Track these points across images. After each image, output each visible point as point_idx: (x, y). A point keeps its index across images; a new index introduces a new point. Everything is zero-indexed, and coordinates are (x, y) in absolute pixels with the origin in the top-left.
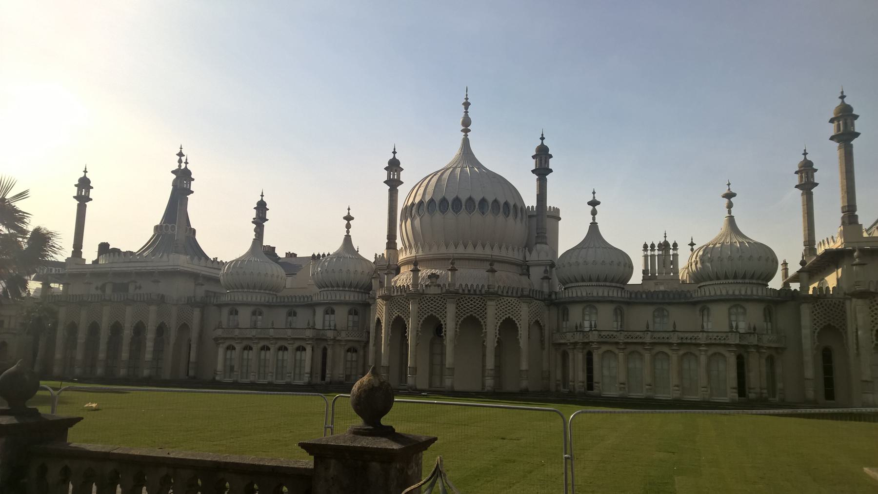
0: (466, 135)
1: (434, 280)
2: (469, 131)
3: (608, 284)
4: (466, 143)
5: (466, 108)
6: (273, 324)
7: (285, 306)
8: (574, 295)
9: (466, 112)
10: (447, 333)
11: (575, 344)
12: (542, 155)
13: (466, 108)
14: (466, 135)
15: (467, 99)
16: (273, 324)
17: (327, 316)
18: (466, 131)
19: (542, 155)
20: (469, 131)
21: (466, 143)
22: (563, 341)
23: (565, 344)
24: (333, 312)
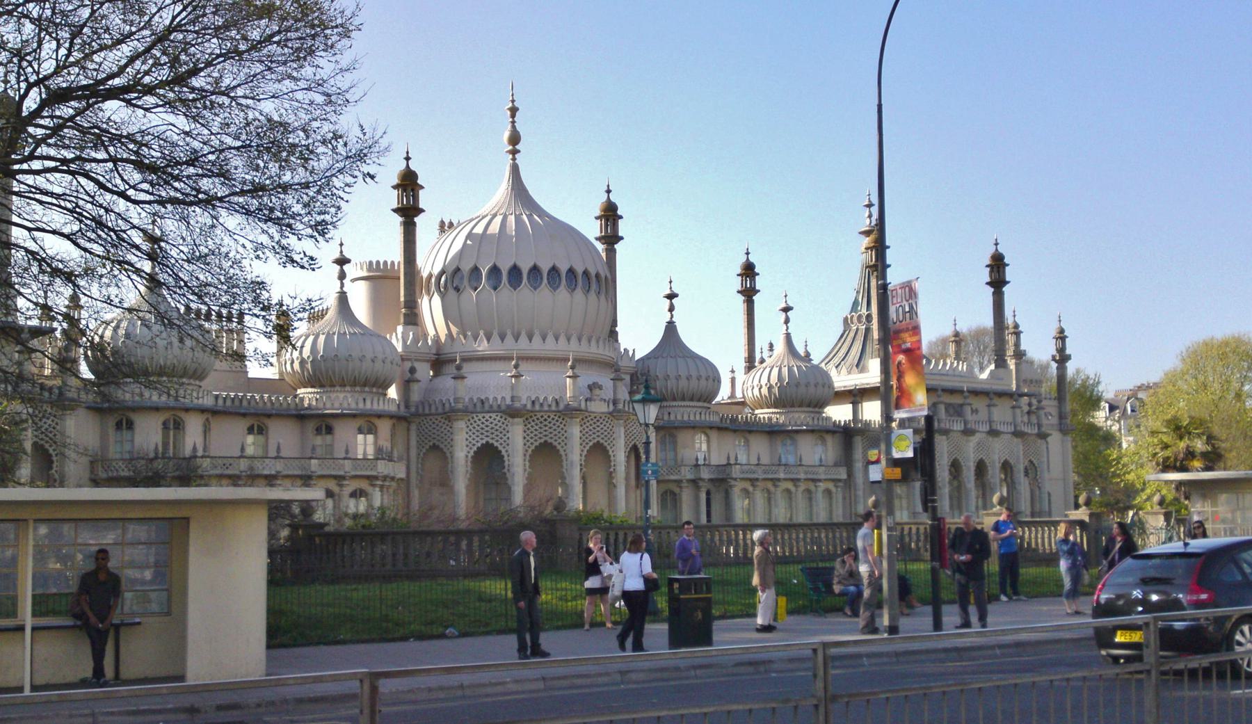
0: (514, 159)
1: (597, 392)
2: (519, 151)
3: (700, 404)
4: (515, 170)
5: (513, 116)
6: (347, 452)
7: (244, 415)
8: (679, 418)
9: (513, 122)
10: (618, 468)
11: (695, 482)
12: (610, 214)
13: (513, 116)
14: (514, 159)
15: (513, 101)
16: (347, 452)
17: (360, 437)
18: (514, 152)
19: (610, 214)
20: (519, 151)
21: (515, 170)
22: (672, 477)
23: (679, 482)
24: (372, 430)
